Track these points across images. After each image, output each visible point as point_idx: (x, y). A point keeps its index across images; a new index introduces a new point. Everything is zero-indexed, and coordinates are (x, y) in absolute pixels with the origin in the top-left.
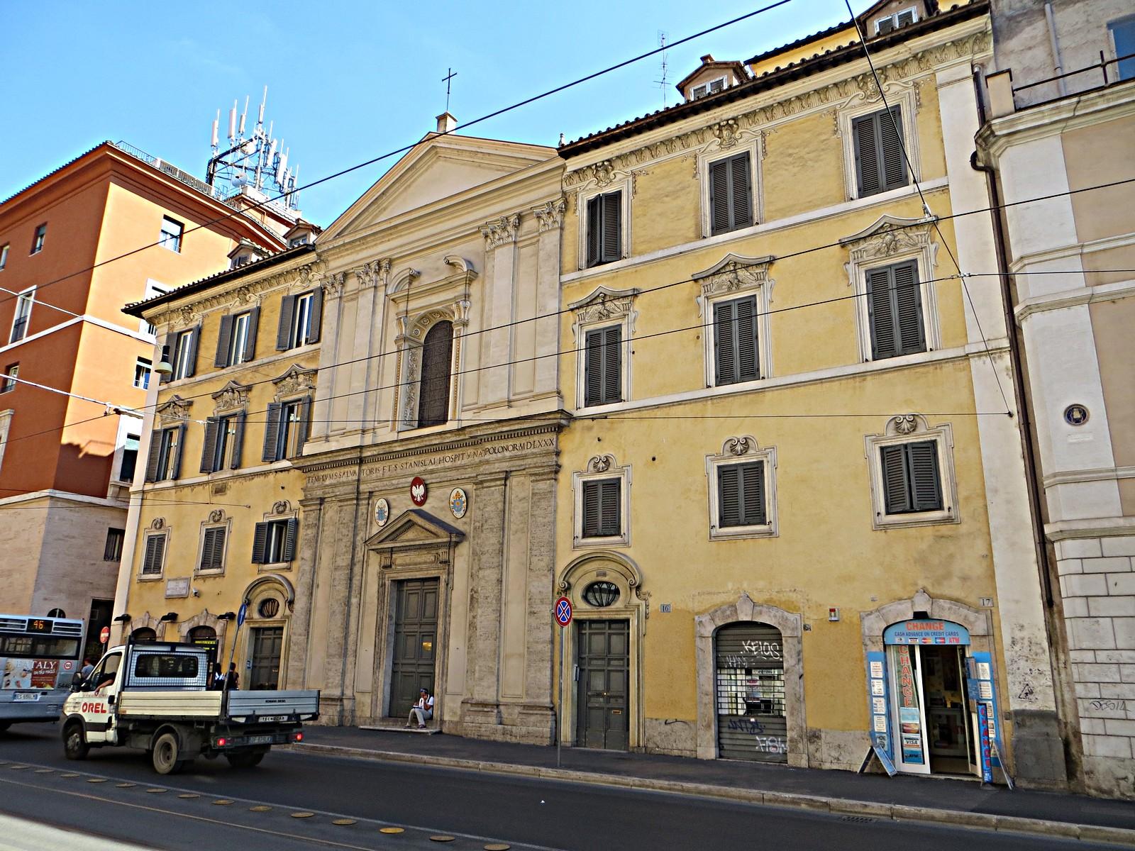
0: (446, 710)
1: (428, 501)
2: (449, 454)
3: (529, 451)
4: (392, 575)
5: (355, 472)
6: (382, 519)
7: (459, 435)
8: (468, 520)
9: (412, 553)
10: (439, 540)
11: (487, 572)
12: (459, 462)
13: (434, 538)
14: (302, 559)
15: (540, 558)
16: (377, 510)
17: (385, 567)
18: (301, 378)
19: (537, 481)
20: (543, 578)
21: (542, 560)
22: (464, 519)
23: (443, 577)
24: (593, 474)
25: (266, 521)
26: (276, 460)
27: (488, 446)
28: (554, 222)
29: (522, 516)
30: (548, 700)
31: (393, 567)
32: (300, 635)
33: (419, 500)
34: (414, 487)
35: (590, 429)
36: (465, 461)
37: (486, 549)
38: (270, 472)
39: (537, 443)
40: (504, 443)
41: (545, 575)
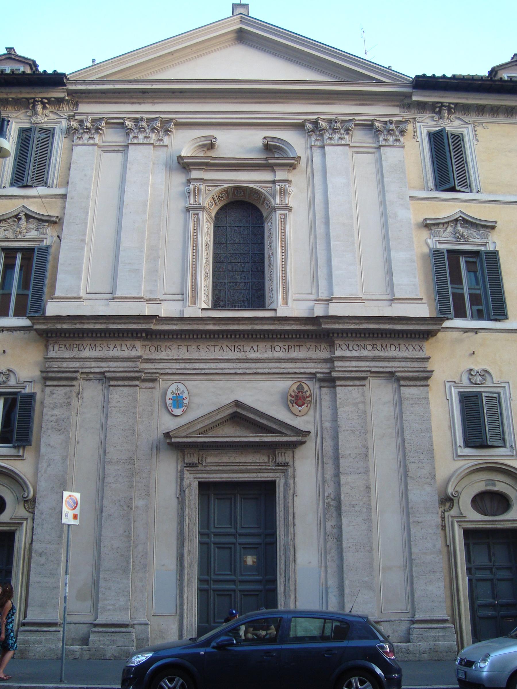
15: (420, 465)
16: (169, 395)
20: (426, 486)
37: (348, 452)
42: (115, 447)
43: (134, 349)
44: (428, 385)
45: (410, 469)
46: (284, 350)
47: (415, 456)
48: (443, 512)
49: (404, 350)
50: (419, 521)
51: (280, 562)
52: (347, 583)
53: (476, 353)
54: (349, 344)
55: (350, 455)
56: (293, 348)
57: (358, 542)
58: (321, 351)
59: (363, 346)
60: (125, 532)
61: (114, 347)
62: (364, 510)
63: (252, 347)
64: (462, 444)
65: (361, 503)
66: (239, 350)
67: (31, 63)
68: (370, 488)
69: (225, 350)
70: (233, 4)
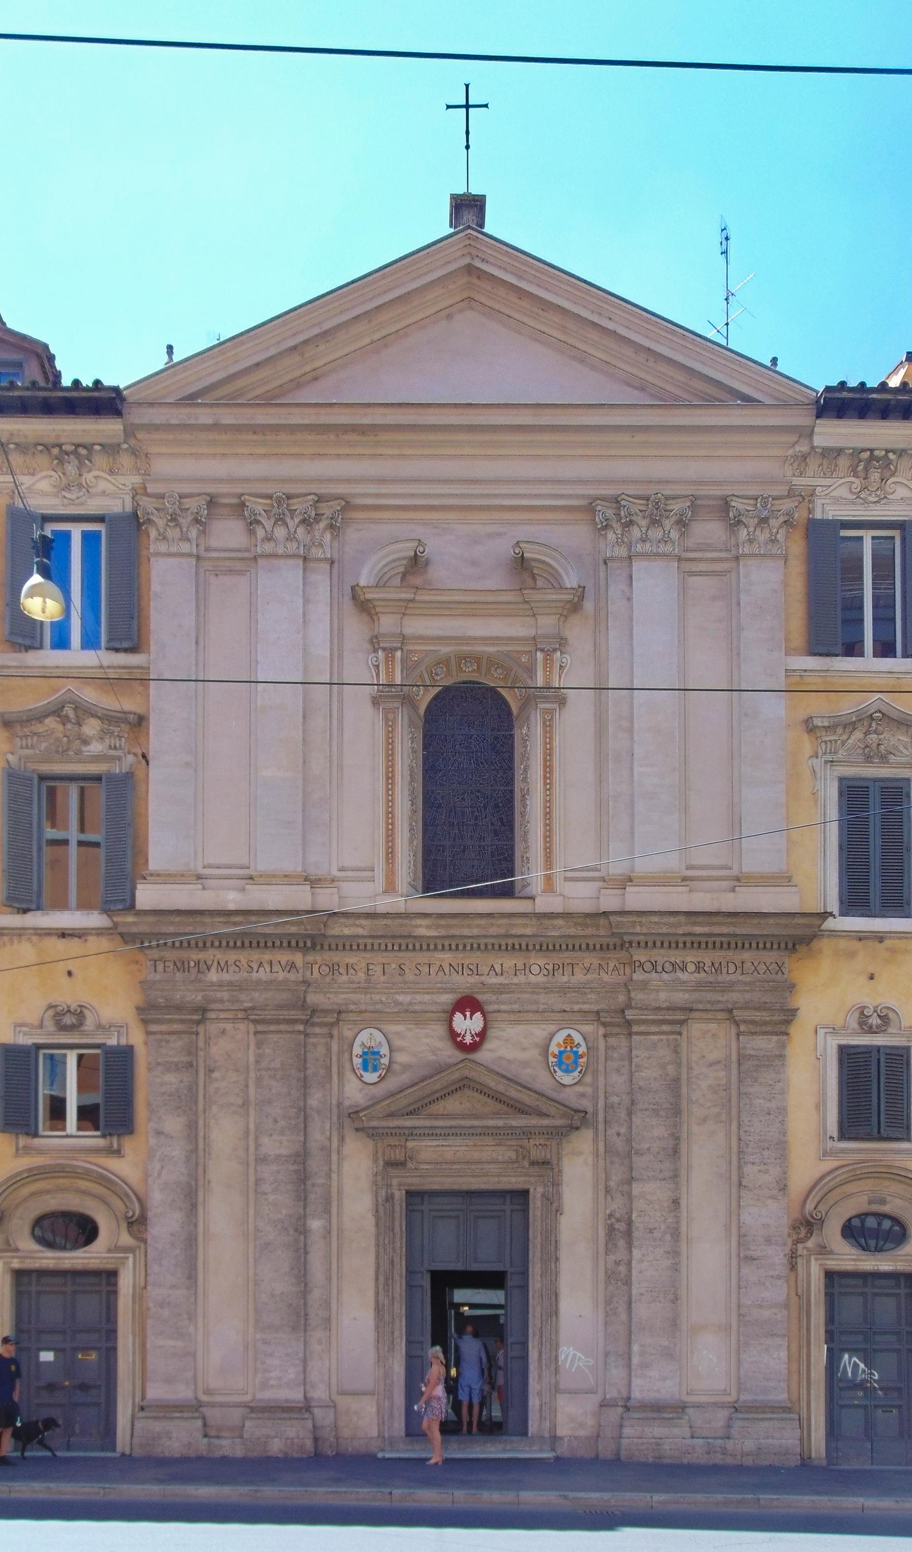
0: (561, 1418)
1: (488, 1045)
2: (538, 961)
3: (732, 977)
4: (409, 1180)
5: (293, 966)
6: (375, 1069)
7: (586, 926)
8: (589, 1090)
9: (458, 1141)
10: (546, 1122)
11: (649, 1187)
12: (565, 979)
13: (496, 1114)
14: (159, 1133)
15: (763, 1167)
16: (357, 1050)
17: (391, 1164)
18: (91, 727)
19: (753, 1034)
20: (769, 1202)
21: (767, 1172)
22: (579, 1089)
23: (537, 1192)
24: (854, 1033)
25: (28, 1041)
26: (38, 908)
27: (640, 956)
28: (774, 541)
29: (715, 1092)
30: (785, 1396)
31: (410, 1165)
32: (174, 1287)
33: (468, 1040)
34: (458, 1017)
35: (852, 955)
36: (580, 977)
37: (646, 1146)
38: (19, 933)
39: (748, 965)
40: (676, 956)
41: (773, 1198)
42: (271, 1135)
43: (293, 970)
44: (787, 1034)
45: (745, 1173)
46: (546, 972)
47: (756, 1153)
48: (797, 1241)
49: (751, 971)
50: (755, 1256)
51: (534, 1316)
52: (636, 1348)
53: (876, 976)
54: (656, 962)
55: (649, 1149)
56: (561, 969)
57: (654, 1287)
58: (610, 973)
59: (681, 965)
60: (293, 1269)
61: (259, 967)
62: (668, 1237)
63: (492, 966)
64: (835, 1134)
65: (663, 1227)
66: (470, 973)
67: (39, 351)
68: (679, 1203)
69: (447, 971)
70: (454, 197)
